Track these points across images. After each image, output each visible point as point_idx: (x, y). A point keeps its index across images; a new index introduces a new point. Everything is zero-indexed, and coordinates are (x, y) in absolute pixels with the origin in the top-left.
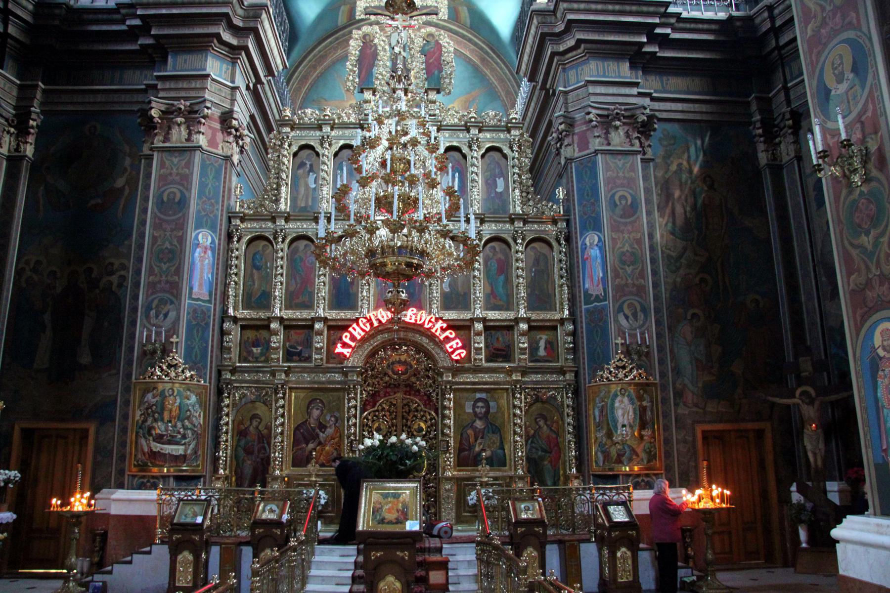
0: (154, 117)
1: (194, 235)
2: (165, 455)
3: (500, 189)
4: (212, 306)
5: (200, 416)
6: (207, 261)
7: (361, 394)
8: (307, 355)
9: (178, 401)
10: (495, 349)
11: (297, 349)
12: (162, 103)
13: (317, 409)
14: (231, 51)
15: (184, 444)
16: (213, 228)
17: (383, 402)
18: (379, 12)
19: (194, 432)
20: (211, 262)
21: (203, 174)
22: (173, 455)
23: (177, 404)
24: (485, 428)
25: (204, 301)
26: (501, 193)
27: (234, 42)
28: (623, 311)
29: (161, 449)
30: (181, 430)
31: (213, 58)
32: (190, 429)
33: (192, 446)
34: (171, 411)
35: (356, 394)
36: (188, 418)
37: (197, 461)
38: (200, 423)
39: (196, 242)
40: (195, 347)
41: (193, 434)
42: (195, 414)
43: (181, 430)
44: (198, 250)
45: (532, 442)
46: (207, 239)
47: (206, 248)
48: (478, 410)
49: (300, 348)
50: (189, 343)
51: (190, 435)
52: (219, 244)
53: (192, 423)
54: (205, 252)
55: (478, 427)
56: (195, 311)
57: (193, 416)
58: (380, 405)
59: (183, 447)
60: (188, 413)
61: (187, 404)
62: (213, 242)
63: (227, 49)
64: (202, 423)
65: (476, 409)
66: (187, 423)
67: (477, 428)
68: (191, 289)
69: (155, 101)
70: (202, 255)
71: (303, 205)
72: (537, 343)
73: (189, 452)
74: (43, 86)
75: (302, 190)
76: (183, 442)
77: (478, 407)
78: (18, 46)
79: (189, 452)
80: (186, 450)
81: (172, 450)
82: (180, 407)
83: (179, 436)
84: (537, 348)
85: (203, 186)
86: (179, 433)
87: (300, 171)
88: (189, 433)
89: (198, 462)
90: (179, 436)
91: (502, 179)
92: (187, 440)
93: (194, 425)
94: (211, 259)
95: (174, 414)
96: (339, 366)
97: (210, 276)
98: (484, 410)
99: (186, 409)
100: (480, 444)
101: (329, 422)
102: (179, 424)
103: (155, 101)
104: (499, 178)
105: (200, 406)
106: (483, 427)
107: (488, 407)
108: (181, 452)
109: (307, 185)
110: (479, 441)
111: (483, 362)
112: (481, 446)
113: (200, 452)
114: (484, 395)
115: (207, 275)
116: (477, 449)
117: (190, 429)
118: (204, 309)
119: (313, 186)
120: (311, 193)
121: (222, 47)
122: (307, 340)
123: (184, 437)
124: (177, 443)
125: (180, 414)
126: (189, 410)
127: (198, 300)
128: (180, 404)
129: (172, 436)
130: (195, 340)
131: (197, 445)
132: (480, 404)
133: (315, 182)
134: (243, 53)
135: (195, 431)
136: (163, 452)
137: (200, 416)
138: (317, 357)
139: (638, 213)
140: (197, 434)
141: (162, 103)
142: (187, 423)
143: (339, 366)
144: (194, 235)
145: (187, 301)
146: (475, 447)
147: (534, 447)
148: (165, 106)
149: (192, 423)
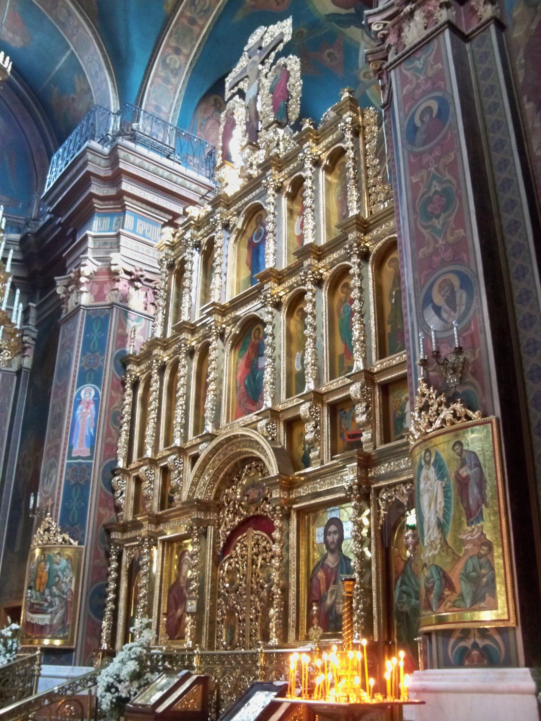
0: (60, 295)
1: (75, 393)
2: (33, 624)
4: (93, 461)
5: (71, 581)
6: (89, 416)
9: (48, 566)
10: (349, 437)
12: (65, 279)
14: (116, 202)
15: (51, 613)
16: (97, 381)
18: (238, 79)
19: (62, 599)
20: (94, 416)
21: (89, 329)
22: (39, 625)
23: (47, 570)
24: (337, 566)
25: (83, 458)
27: (112, 192)
28: (432, 301)
29: (32, 619)
30: (49, 598)
31: (99, 216)
32: (59, 596)
33: (58, 615)
34: (41, 577)
36: (57, 584)
37: (64, 632)
38: (70, 590)
39: (78, 399)
40: (72, 507)
41: (61, 602)
42: (65, 580)
43: (49, 598)
44: (80, 407)
45: (403, 583)
46: (90, 394)
47: (89, 403)
48: (330, 538)
50: (66, 504)
51: (57, 603)
52: (103, 395)
53: (60, 589)
54: (87, 408)
55: (330, 564)
56: (75, 470)
57: (63, 582)
59: (48, 617)
60: (57, 579)
61: (56, 569)
62: (97, 395)
63: (111, 202)
64: (73, 588)
66: (54, 589)
67: (329, 567)
68: (71, 448)
69: (59, 280)
70: (84, 410)
73: (55, 621)
74: (34, 305)
76: (50, 610)
78: (22, 281)
79: (55, 621)
80: (51, 620)
81: (39, 619)
82: (49, 573)
83: (46, 604)
85: (87, 342)
86: (46, 600)
88: (57, 600)
89: (67, 633)
90: (46, 604)
92: (54, 609)
93: (63, 593)
94: (94, 412)
95: (43, 580)
97: (92, 431)
99: (54, 575)
100: (333, 592)
102: (47, 592)
103: (59, 280)
105: (72, 569)
106: (336, 564)
108: (47, 622)
110: (331, 588)
112: (334, 597)
113: (68, 622)
115: (89, 430)
116: (329, 602)
117: (59, 596)
118: (84, 466)
121: (107, 203)
123: (51, 605)
124: (44, 612)
125: (48, 580)
126: (58, 576)
127: (79, 457)
128: (49, 569)
129: (41, 605)
130: (73, 500)
131: (65, 614)
134: (125, 198)
135: (64, 599)
136: (32, 622)
137: (71, 581)
139: (450, 119)
140: (67, 602)
141: (65, 279)
142: (54, 589)
144: (75, 393)
145: (66, 461)
146: (326, 599)
147: (404, 592)
148: (67, 280)
149: (60, 589)
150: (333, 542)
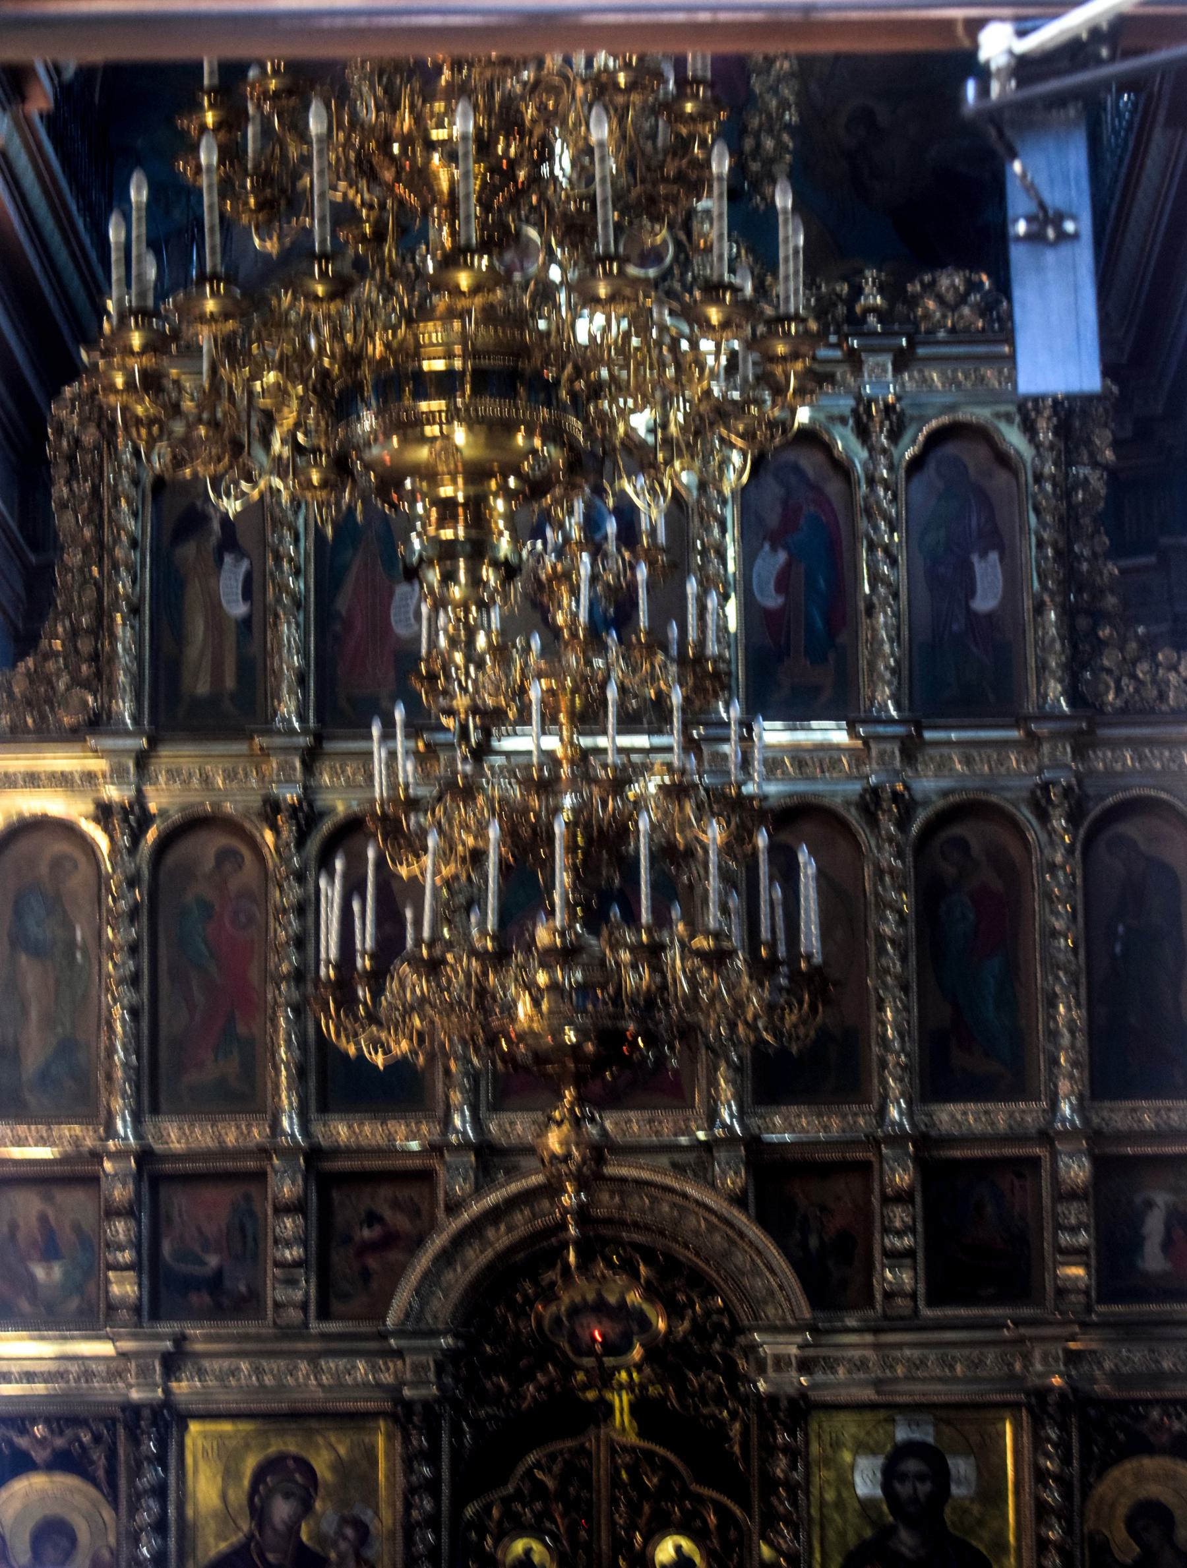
3: (985, 601)
7: (457, 1432)
8: (243, 1288)
11: (203, 1263)
13: (287, 1496)
17: (538, 1465)
26: (990, 616)
35: (435, 1441)
49: (213, 1261)
55: (904, 1550)
58: (529, 1473)
65: (898, 1486)
71: (203, 688)
72: (1135, 1220)
75: (198, 628)
77: (903, 1477)
84: (1136, 1243)
87: (188, 550)
91: (994, 556)
96: (365, 1327)
98: (924, 1488)
101: (335, 1544)
104: (983, 555)
107: (941, 1477)
109: (214, 609)
111: (921, 1303)
114: (926, 1434)
119: (239, 609)
120: (231, 640)
122: (243, 1230)
132: (912, 1466)
133: (247, 594)
138: (281, 1295)
143: (365, 1327)
150: (914, 1499)
